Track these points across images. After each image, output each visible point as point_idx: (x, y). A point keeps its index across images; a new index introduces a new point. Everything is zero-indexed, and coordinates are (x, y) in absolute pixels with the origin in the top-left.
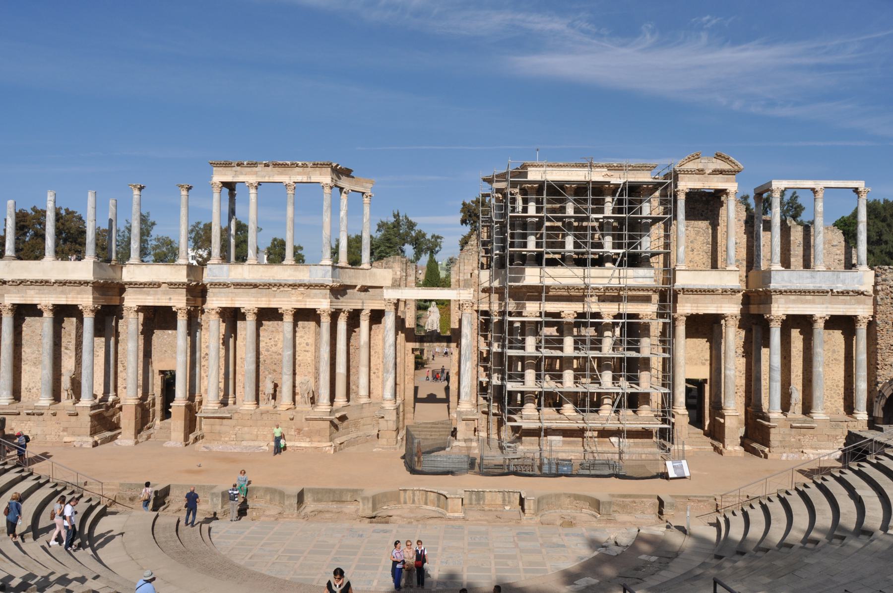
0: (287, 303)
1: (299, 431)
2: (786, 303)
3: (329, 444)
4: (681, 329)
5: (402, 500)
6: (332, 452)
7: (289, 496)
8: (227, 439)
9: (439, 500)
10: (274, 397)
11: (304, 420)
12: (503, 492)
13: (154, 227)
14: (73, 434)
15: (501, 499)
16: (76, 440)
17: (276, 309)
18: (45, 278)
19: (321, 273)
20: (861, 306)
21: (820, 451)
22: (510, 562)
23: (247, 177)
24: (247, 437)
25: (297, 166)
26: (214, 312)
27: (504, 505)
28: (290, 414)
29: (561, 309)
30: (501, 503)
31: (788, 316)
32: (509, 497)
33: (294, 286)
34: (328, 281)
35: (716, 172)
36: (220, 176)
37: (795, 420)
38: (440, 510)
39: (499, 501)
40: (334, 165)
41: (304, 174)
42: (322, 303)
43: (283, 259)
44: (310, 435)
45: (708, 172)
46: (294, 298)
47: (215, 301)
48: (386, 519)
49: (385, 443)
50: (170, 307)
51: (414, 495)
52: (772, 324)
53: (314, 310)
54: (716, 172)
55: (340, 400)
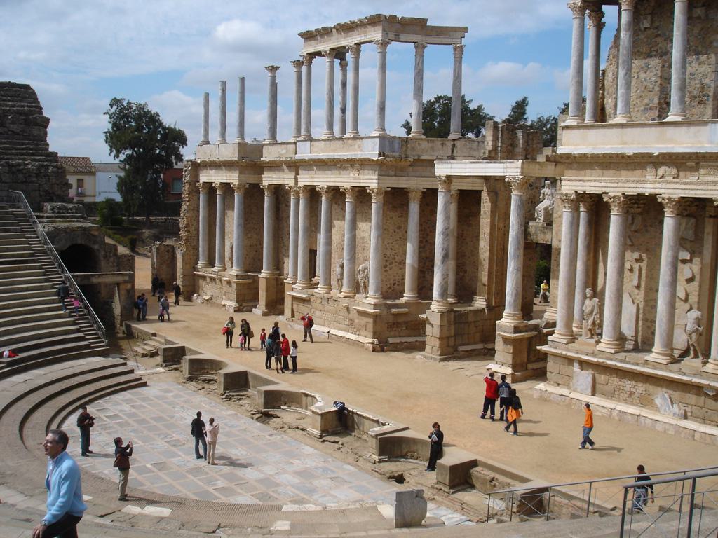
0: (347, 180)
1: (352, 321)
5: (304, 403)
6: (371, 349)
28: (345, 303)
29: (604, 190)
42: (370, 181)
44: (357, 330)
50: (284, 185)
55: (408, 296)
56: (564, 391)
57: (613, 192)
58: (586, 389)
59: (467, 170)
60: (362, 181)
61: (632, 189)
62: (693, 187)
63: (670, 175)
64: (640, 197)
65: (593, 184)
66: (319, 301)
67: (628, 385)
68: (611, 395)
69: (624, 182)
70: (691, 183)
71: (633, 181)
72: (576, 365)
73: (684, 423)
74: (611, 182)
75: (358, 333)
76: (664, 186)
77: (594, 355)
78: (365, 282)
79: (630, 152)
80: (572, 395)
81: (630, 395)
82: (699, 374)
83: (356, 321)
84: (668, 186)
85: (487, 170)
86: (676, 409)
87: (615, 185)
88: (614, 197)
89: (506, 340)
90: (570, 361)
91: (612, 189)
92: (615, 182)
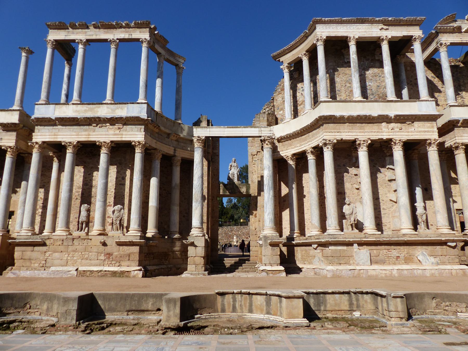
0: (104, 135)
1: (109, 255)
3: (139, 268)
7: (66, 300)
8: (36, 265)
9: (268, 303)
11: (114, 244)
12: (348, 293)
15: (347, 303)
19: (139, 110)
23: (79, 35)
24: (56, 262)
25: (121, 27)
26: (37, 146)
27: (351, 311)
30: (347, 308)
32: (357, 300)
34: (144, 115)
36: (55, 35)
38: (272, 317)
39: (345, 306)
40: (152, 26)
41: (127, 32)
42: (136, 135)
45: (463, 30)
46: (111, 132)
48: (200, 329)
49: (194, 269)
51: (234, 300)
57: (362, 138)
58: (367, 261)
59: (226, 133)
60: (124, 136)
61: (376, 136)
62: (413, 134)
63: (397, 128)
65: (347, 134)
66: (60, 243)
68: (383, 262)
69: (368, 132)
70: (412, 132)
71: (375, 132)
72: (356, 245)
74: (360, 132)
75: (118, 264)
76: (394, 134)
77: (365, 237)
78: (121, 220)
80: (358, 268)
81: (397, 259)
83: (115, 254)
84: (397, 134)
85: (244, 132)
86: (432, 260)
87: (363, 134)
88: (364, 141)
91: (361, 137)
92: (362, 132)
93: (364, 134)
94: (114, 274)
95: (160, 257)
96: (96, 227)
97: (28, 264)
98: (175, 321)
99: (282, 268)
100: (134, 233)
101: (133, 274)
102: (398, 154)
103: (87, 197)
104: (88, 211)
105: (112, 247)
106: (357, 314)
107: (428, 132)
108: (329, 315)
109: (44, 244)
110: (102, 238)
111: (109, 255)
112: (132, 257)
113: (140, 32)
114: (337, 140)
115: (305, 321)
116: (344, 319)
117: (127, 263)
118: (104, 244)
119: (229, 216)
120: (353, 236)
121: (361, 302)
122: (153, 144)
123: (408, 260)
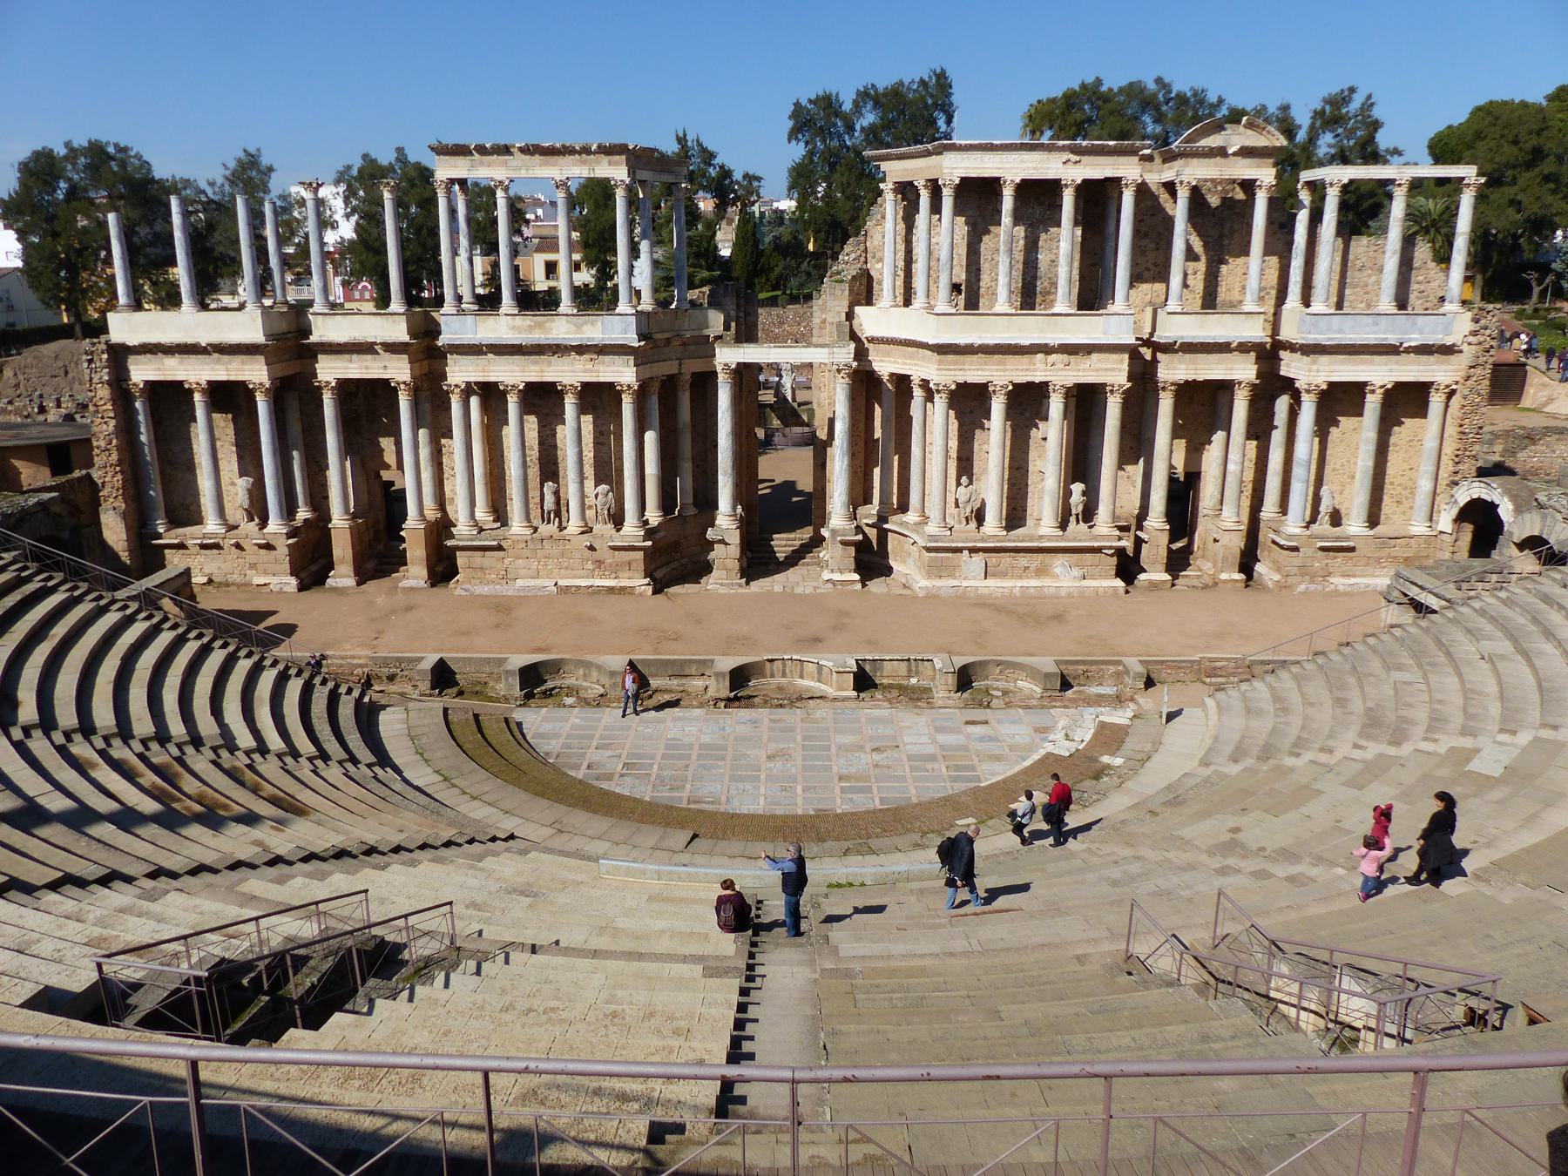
0: (569, 373)
2: (1331, 363)
4: (1166, 404)
10: (558, 514)
13: (273, 175)
14: (265, 573)
16: (274, 581)
17: (554, 384)
18: (190, 340)
20: (1443, 367)
21: (1353, 580)
22: (929, 766)
24: (522, 572)
28: (586, 540)
31: (1331, 384)
33: (581, 349)
34: (632, 339)
35: (1247, 152)
37: (1323, 538)
38: (823, 687)
41: (584, 163)
42: (623, 373)
43: (557, 305)
47: (460, 372)
51: (784, 666)
52: (1305, 397)
53: (611, 385)
54: (1247, 152)
56: (955, 583)
61: (1022, 378)
64: (1030, 385)
67: (1023, 560)
72: (966, 552)
73: (1085, 583)
77: (983, 540)
79: (1027, 343)
80: (965, 584)
82: (1095, 538)
86: (1076, 572)
89: (845, 543)
90: (959, 550)
93: (1001, 375)
94: (611, 590)
95: (675, 559)
96: (574, 525)
97: (480, 574)
98: (725, 692)
99: (857, 577)
100: (631, 529)
101: (638, 590)
102: (1056, 405)
103: (549, 468)
104: (557, 493)
105: (603, 552)
106: (914, 681)
107: (1112, 370)
108: (885, 681)
109: (499, 548)
110: (586, 540)
111: (599, 563)
112: (634, 566)
113: (610, 164)
114: (958, 385)
115: (855, 694)
116: (899, 687)
117: (628, 574)
118: (591, 548)
119: (773, 276)
120: (963, 536)
121: (921, 668)
122: (650, 371)
123: (1041, 572)
